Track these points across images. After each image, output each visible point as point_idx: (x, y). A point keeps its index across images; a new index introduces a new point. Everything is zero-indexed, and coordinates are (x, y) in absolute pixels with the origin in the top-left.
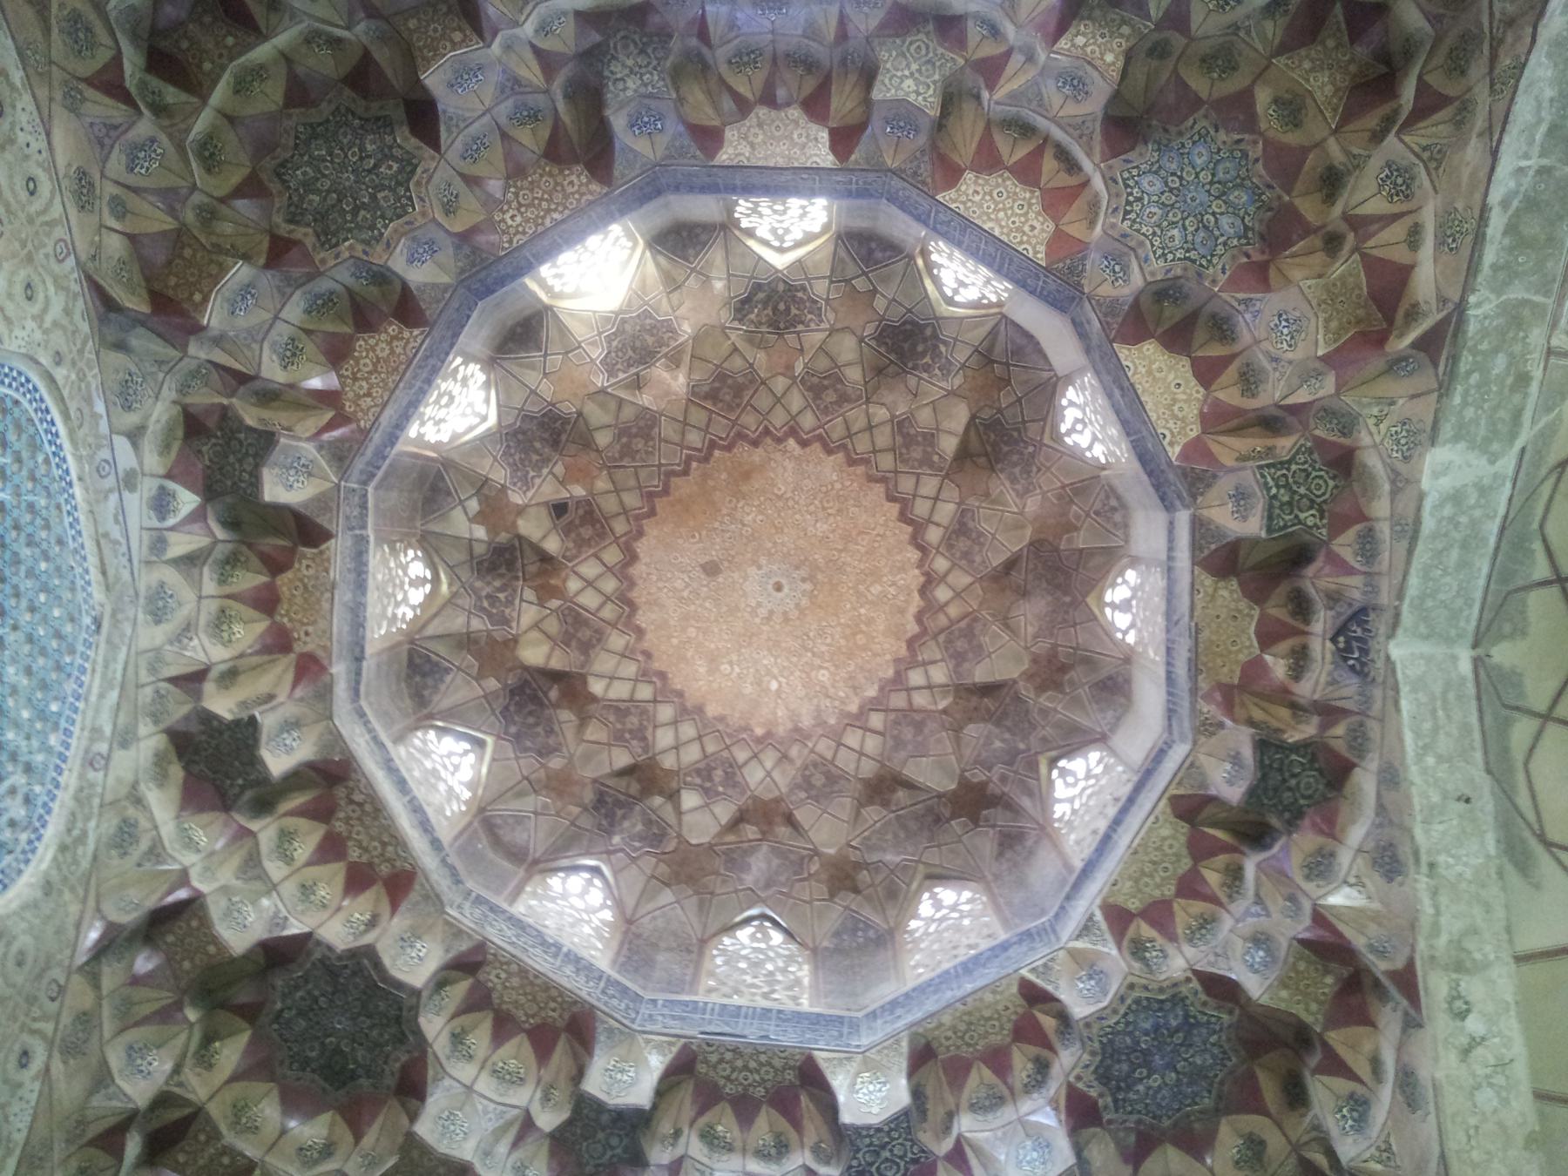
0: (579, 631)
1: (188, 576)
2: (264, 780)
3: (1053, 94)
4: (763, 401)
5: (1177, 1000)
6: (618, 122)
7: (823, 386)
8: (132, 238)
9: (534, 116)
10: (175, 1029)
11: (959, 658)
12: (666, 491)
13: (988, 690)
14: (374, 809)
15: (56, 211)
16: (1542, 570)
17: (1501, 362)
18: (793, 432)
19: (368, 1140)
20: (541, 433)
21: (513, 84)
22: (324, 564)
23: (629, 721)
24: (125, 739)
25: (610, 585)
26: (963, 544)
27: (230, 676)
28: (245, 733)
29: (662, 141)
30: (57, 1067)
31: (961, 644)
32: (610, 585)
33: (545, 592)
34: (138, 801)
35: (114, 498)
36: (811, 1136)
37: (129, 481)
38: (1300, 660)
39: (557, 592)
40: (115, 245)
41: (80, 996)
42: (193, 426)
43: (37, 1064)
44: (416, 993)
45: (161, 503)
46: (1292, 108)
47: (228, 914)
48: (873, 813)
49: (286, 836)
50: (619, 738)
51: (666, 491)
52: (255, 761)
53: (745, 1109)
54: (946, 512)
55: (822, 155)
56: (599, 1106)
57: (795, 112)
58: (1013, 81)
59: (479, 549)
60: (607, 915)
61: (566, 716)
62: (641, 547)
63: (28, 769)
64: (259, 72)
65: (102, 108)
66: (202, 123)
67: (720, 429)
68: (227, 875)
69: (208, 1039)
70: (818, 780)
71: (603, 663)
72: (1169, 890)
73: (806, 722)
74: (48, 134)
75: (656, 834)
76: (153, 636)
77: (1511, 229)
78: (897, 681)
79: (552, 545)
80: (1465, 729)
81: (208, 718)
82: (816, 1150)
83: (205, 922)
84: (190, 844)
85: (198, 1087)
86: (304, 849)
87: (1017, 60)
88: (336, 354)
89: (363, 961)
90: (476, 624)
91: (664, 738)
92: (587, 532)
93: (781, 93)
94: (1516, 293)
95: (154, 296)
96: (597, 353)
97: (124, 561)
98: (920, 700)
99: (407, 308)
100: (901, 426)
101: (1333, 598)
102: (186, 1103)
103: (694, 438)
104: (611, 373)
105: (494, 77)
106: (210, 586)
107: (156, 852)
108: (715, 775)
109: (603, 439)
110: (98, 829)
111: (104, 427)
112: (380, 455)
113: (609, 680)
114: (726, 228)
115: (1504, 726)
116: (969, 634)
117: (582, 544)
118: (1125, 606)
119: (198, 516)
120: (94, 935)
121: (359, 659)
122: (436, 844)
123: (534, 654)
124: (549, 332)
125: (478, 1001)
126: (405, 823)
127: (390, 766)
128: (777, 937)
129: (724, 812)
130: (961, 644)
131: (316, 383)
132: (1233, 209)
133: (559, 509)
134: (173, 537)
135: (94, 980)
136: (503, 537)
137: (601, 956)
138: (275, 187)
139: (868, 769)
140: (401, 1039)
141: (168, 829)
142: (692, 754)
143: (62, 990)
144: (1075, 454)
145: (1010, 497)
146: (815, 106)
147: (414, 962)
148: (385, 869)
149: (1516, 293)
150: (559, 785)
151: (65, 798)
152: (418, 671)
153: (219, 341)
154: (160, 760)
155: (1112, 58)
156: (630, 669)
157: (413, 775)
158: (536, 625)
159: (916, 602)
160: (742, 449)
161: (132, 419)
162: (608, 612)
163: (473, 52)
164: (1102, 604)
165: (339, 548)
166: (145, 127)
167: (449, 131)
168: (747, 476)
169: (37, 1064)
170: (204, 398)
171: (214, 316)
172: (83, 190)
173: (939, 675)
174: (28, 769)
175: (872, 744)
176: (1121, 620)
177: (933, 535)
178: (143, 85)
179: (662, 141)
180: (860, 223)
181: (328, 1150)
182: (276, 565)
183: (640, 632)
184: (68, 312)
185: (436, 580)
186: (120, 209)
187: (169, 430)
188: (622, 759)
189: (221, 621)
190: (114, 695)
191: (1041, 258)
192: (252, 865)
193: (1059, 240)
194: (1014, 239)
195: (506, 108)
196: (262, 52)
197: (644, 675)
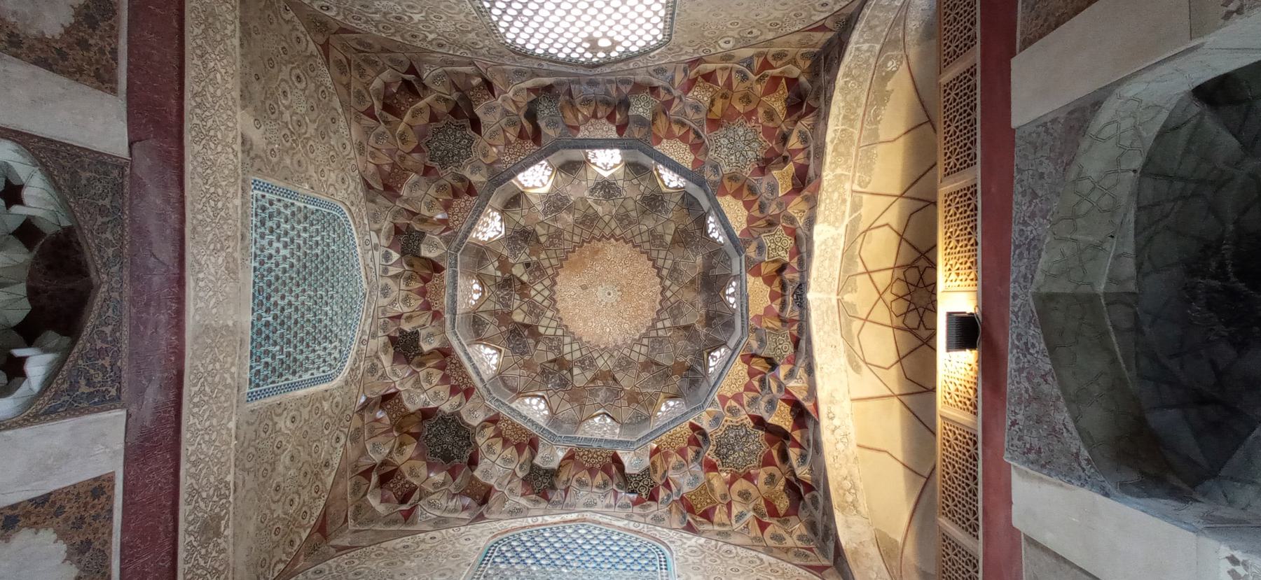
0: (535, 310)
2: (421, 354)
3: (689, 112)
4: (601, 225)
5: (743, 425)
6: (542, 124)
7: (624, 219)
8: (377, 165)
9: (514, 124)
11: (674, 317)
12: (567, 259)
13: (686, 328)
14: (460, 365)
15: (352, 155)
16: (861, 269)
17: (836, 195)
18: (613, 236)
19: (458, 481)
20: (521, 237)
21: (506, 113)
22: (442, 279)
23: (555, 343)
24: (374, 336)
25: (546, 293)
26: (676, 275)
27: (409, 318)
28: (415, 335)
29: (558, 131)
30: (349, 444)
31: (676, 312)
32: (546, 293)
33: (523, 295)
34: (378, 358)
36: (616, 480)
37: (376, 247)
38: (783, 305)
39: (528, 296)
40: (371, 168)
41: (356, 422)
42: (397, 230)
43: (343, 441)
44: (475, 428)
45: (387, 257)
46: (770, 115)
47: (408, 398)
48: (645, 375)
49: (429, 375)
50: (550, 349)
51: (567, 259)
52: (418, 346)
53: (592, 472)
54: (669, 263)
55: (614, 135)
56: (539, 468)
57: (604, 121)
58: (675, 107)
59: (498, 280)
60: (546, 412)
61: (531, 341)
62: (557, 279)
63: (341, 341)
64: (420, 111)
65: (368, 121)
66: (401, 127)
67: (586, 235)
68: (408, 386)
69: (401, 445)
70: (624, 364)
71: (544, 322)
72: (742, 389)
73: (620, 343)
75: (564, 384)
76: (384, 302)
77: (835, 150)
78: (653, 327)
79: (525, 278)
80: (834, 322)
81: (402, 331)
82: (618, 485)
83: (400, 400)
84: (395, 374)
85: (398, 459)
86: (435, 380)
87: (677, 101)
88: (447, 206)
89: (455, 416)
90: (497, 307)
91: (567, 349)
92: (537, 274)
93: (599, 115)
94: (839, 171)
95: (385, 186)
96: (540, 208)
98: (660, 333)
99: (471, 190)
100: (651, 232)
101: (792, 281)
102: (393, 465)
103: (576, 239)
104: (546, 215)
105: (499, 110)
106: (403, 286)
107: (383, 376)
108: (586, 362)
109: (543, 239)
110: (364, 366)
112: (462, 242)
113: (546, 327)
114: (585, 163)
115: (849, 324)
116: (678, 308)
117: (536, 278)
118: (732, 295)
119: (399, 262)
120: (363, 400)
121: (455, 314)
122: (482, 380)
123: (518, 317)
124: (523, 201)
125: (498, 434)
126: (470, 370)
127: (466, 354)
128: (609, 420)
129: (589, 375)
130: (676, 312)
131: (440, 216)
132: (752, 149)
133: (528, 265)
134: (390, 268)
135: (362, 418)
136: (507, 275)
137: (542, 423)
138: (426, 149)
139: (642, 359)
140: (469, 445)
141: (388, 369)
142: (577, 355)
144: (714, 240)
145: (691, 257)
146: (611, 118)
147: (474, 417)
148: (464, 387)
149: (839, 171)
150: (527, 366)
151: (353, 353)
152: (476, 323)
153: (406, 201)
154: (385, 345)
155: (706, 99)
156: (554, 324)
157: (475, 359)
158: (519, 307)
159: (660, 297)
160: (594, 243)
161: (377, 226)
162: (546, 303)
163: (492, 102)
164: (725, 295)
165: (447, 273)
166: (382, 128)
168: (596, 252)
169: (343, 441)
170: (401, 221)
171: (405, 192)
172: (361, 149)
173: (668, 323)
174: (341, 341)
175: (644, 350)
176: (732, 300)
177: (665, 272)
178: (381, 115)
179: (558, 131)
180: (631, 160)
181: (444, 484)
182: (426, 280)
183: (558, 311)
185: (483, 292)
186: (373, 155)
187: (389, 231)
188: (551, 356)
189: (406, 300)
190: (370, 320)
191: (690, 168)
192: (417, 382)
193: (695, 161)
194: (680, 162)
195: (505, 120)
196: (421, 104)
197: (559, 326)
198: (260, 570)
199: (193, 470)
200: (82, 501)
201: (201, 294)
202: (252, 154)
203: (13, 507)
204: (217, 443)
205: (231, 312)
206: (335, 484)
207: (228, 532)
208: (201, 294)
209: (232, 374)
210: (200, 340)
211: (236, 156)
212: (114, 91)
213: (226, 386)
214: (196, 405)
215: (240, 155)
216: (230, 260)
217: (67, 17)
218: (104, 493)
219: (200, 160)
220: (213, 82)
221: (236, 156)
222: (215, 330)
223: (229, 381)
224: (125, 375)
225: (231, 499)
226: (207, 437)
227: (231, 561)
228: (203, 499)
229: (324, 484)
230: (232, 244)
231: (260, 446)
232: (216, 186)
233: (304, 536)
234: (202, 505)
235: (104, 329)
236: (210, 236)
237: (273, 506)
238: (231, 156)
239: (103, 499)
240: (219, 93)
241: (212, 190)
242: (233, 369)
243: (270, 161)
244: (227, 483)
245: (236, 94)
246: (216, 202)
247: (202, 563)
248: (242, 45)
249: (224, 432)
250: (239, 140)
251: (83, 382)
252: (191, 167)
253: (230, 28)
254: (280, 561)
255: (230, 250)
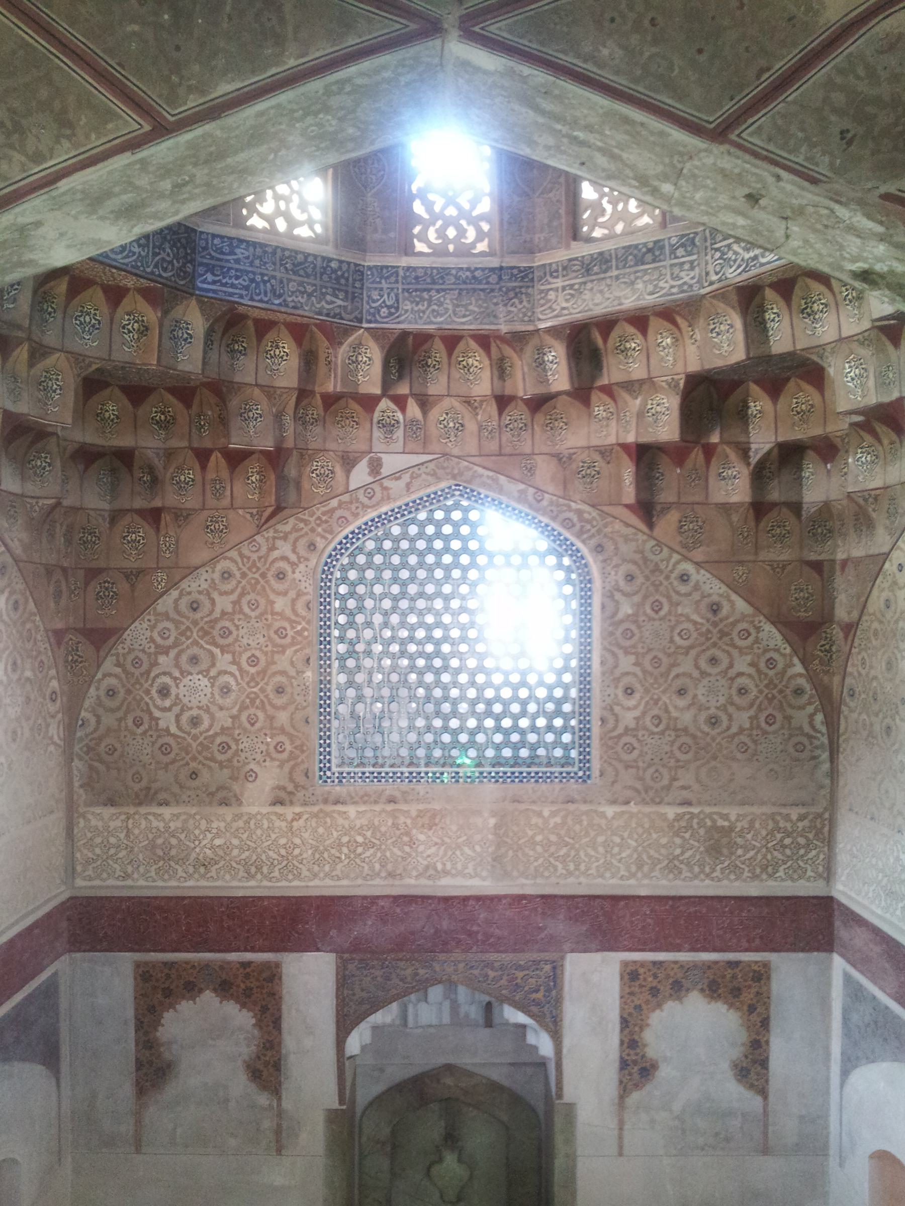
1: (435, 403)
10: (719, 449)
15: (234, 554)
30: (699, 554)
35: (386, 483)
37: (375, 467)
74: (197, 568)
97: (423, 468)
111: (346, 498)
143: (659, 544)
167: (90, 365)
169: (689, 567)
184: (285, 538)
190: (502, 479)
198: (806, 755)
199: (646, 869)
200: (637, 990)
201: (459, 866)
202: (290, 788)
203: (622, 1043)
204: (626, 835)
205: (479, 821)
206: (749, 595)
207: (733, 812)
208: (459, 866)
209: (554, 814)
210: (509, 868)
211: (299, 816)
212: (278, 965)
213: (564, 823)
214: (577, 868)
215: (298, 809)
216: (420, 822)
217: (231, 1008)
218: (636, 970)
219: (316, 868)
220: (227, 848)
221: (299, 816)
222: (498, 846)
223: (558, 820)
224: (536, 956)
225: (695, 810)
226: (616, 850)
227: (767, 809)
228: (682, 853)
229: (743, 617)
230: (402, 819)
231: (648, 758)
232: (341, 845)
233: (799, 668)
234: (687, 855)
235: (490, 978)
236: (396, 850)
237: (734, 730)
238: (301, 822)
239: (641, 971)
240: (235, 842)
241: (345, 850)
242: (546, 813)
243: (292, 756)
244: (679, 817)
245: (227, 813)
246: (359, 845)
247: (752, 853)
248: (166, 803)
249: (616, 823)
250: (279, 809)
251: (534, 996)
252: (328, 882)
253: (155, 823)
254: (811, 716)
255: (409, 822)
